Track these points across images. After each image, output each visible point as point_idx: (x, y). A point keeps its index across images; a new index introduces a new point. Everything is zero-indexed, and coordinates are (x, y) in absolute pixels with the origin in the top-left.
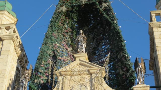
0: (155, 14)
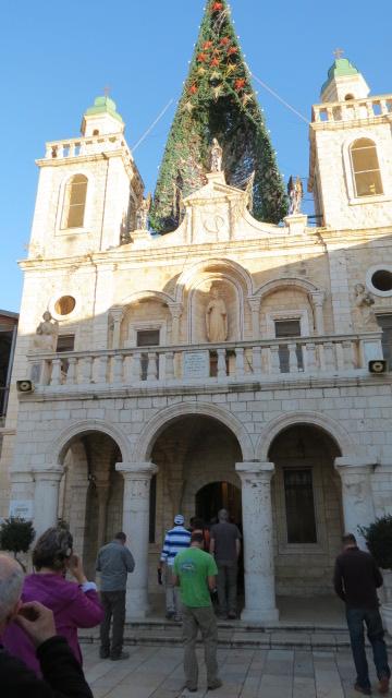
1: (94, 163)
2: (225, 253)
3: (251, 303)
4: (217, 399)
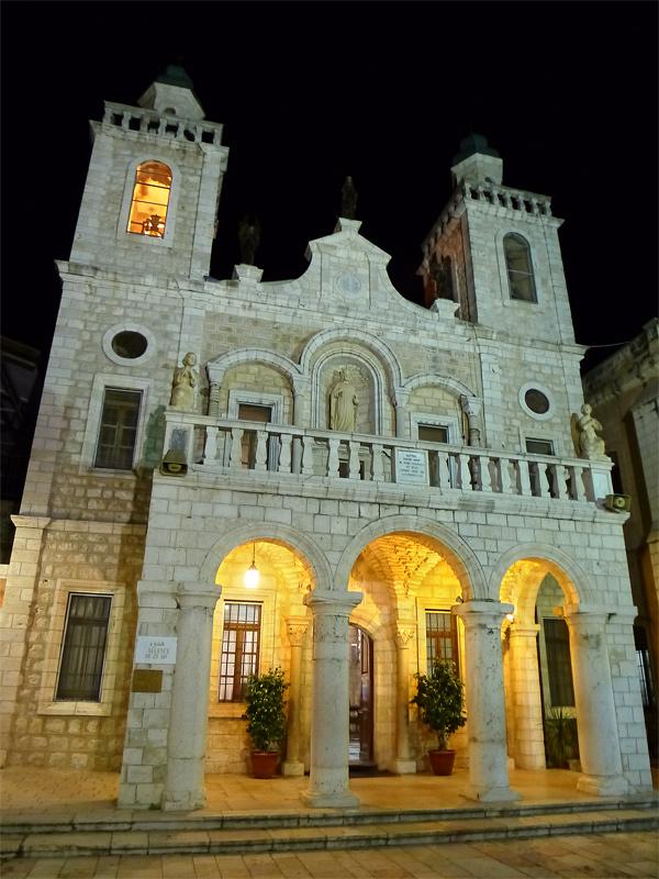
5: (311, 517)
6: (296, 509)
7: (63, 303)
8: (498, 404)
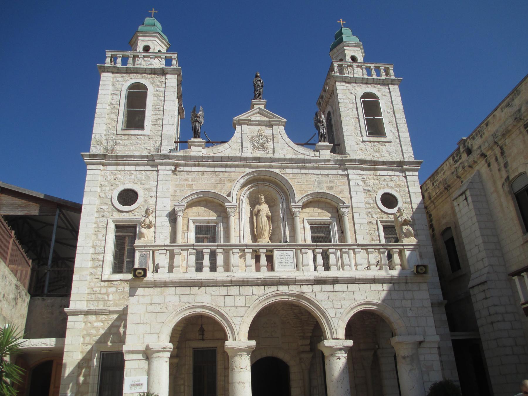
0: (337, 65)
1: (153, 76)
2: (271, 167)
3: (294, 210)
4: (306, 289)
5: (222, 298)
6: (213, 293)
7: (88, 178)
8: (362, 205)
